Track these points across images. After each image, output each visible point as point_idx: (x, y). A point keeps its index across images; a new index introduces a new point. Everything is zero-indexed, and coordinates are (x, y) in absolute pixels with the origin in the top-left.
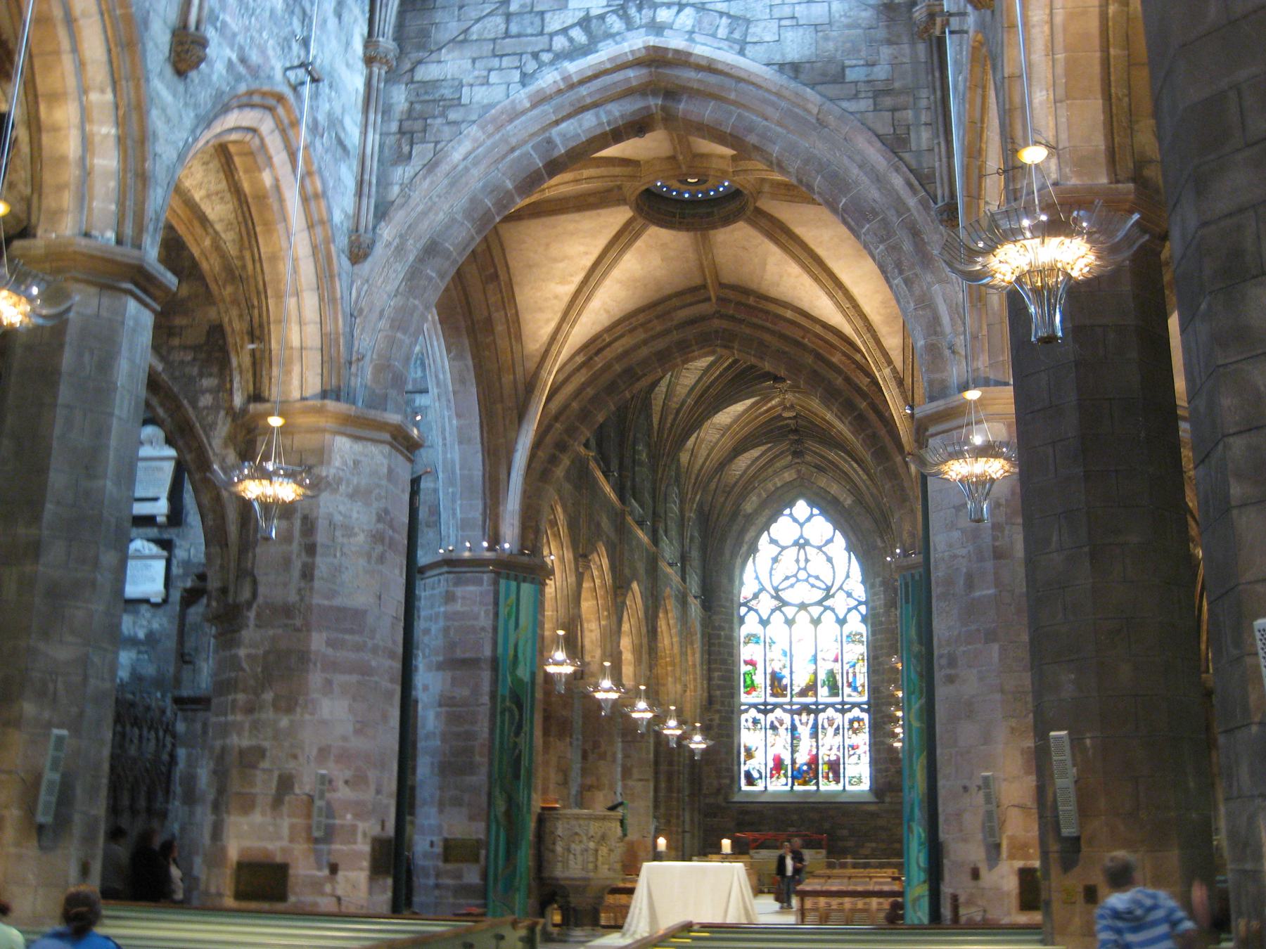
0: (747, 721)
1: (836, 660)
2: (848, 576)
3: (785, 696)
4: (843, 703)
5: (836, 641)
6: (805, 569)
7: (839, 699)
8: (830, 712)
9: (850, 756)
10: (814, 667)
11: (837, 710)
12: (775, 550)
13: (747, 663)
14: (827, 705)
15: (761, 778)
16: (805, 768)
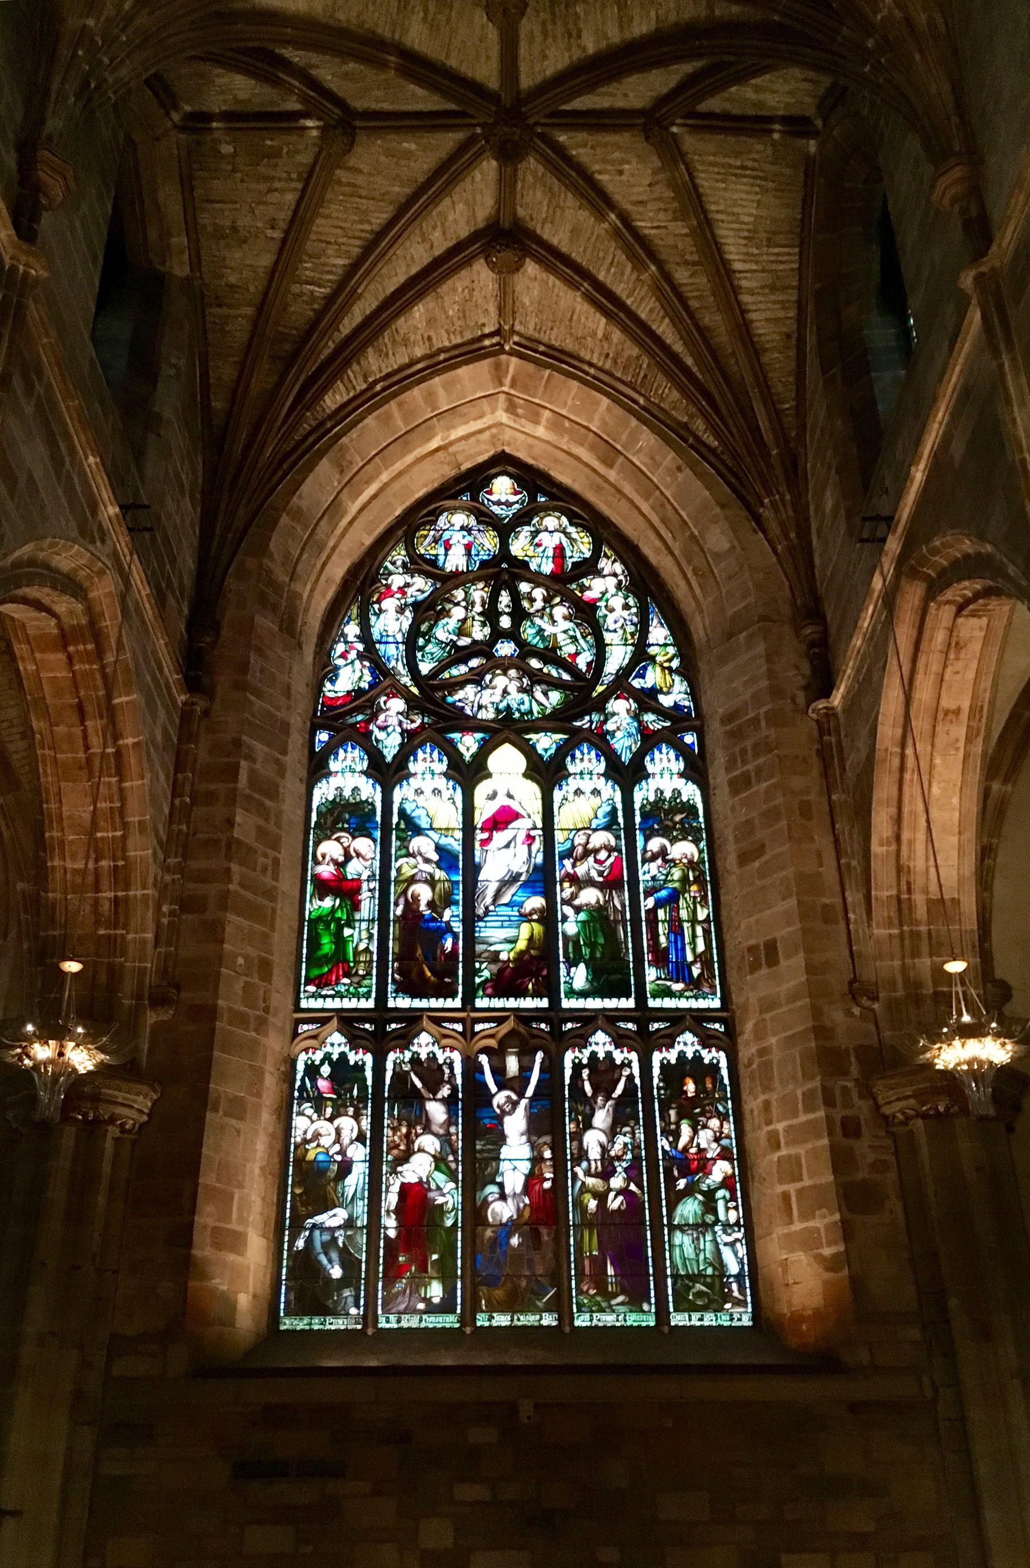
0: (312, 1070)
1: (610, 883)
2: (641, 656)
3: (453, 995)
4: (642, 1014)
5: (610, 826)
6: (513, 635)
7: (629, 1003)
8: (601, 1043)
9: (676, 1198)
10: (537, 902)
11: (620, 1040)
12: (421, 586)
13: (323, 888)
14: (589, 1021)
15: (350, 1278)
16: (515, 1241)
